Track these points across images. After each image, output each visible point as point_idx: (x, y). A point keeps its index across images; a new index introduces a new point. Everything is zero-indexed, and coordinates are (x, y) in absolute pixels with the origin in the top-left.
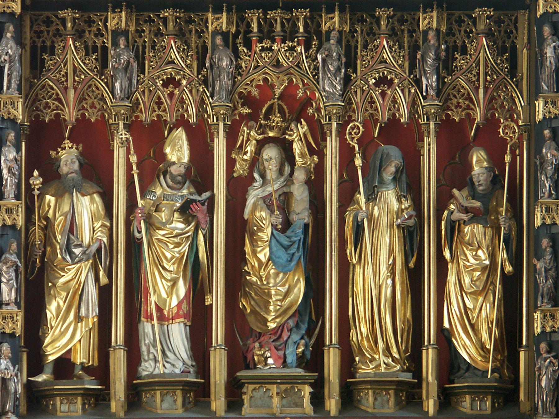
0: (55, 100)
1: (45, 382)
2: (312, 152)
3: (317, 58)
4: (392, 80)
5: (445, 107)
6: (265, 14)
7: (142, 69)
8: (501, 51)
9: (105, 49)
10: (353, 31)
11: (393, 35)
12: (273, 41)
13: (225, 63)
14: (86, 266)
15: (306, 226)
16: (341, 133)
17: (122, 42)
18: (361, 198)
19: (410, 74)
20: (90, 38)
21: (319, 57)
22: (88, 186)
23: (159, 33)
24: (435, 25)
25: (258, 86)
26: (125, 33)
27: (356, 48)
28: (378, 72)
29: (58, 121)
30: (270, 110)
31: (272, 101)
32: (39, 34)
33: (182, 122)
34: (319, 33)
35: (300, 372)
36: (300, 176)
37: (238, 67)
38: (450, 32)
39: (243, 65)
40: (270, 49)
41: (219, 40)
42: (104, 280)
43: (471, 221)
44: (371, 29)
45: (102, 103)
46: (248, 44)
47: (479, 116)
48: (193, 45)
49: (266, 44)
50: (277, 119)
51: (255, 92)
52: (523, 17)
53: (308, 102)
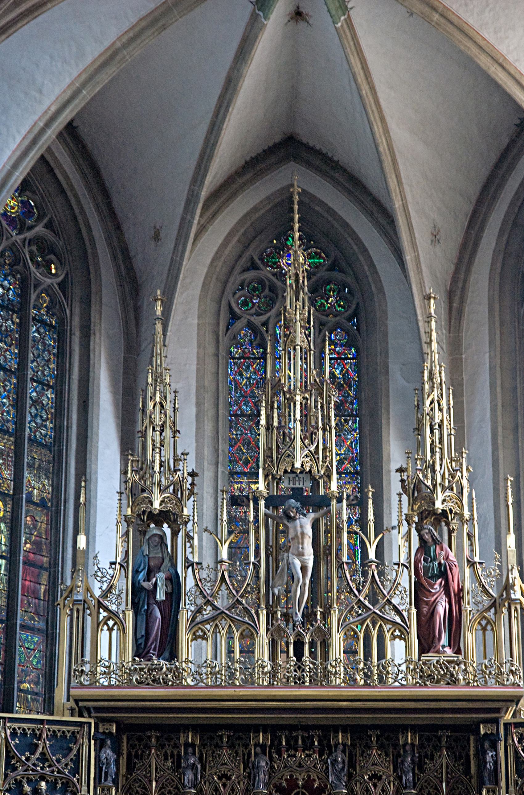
0: (142, 788)
3: (327, 762)
4: (381, 776)
6: (291, 733)
7: (204, 768)
8: (457, 759)
9: (179, 755)
11: (381, 747)
12: (296, 750)
13: (263, 763)
17: (190, 750)
19: (394, 772)
21: (329, 761)
24: (410, 741)
25: (286, 780)
26: (193, 745)
27: (356, 756)
28: (371, 771)
31: (298, 790)
32: (133, 747)
34: (329, 747)
37: (272, 767)
38: (422, 746)
39: (276, 766)
40: (294, 756)
41: (258, 749)
44: (367, 743)
45: (176, 790)
48: (241, 753)
49: (292, 752)
51: (284, 784)
52: (472, 738)
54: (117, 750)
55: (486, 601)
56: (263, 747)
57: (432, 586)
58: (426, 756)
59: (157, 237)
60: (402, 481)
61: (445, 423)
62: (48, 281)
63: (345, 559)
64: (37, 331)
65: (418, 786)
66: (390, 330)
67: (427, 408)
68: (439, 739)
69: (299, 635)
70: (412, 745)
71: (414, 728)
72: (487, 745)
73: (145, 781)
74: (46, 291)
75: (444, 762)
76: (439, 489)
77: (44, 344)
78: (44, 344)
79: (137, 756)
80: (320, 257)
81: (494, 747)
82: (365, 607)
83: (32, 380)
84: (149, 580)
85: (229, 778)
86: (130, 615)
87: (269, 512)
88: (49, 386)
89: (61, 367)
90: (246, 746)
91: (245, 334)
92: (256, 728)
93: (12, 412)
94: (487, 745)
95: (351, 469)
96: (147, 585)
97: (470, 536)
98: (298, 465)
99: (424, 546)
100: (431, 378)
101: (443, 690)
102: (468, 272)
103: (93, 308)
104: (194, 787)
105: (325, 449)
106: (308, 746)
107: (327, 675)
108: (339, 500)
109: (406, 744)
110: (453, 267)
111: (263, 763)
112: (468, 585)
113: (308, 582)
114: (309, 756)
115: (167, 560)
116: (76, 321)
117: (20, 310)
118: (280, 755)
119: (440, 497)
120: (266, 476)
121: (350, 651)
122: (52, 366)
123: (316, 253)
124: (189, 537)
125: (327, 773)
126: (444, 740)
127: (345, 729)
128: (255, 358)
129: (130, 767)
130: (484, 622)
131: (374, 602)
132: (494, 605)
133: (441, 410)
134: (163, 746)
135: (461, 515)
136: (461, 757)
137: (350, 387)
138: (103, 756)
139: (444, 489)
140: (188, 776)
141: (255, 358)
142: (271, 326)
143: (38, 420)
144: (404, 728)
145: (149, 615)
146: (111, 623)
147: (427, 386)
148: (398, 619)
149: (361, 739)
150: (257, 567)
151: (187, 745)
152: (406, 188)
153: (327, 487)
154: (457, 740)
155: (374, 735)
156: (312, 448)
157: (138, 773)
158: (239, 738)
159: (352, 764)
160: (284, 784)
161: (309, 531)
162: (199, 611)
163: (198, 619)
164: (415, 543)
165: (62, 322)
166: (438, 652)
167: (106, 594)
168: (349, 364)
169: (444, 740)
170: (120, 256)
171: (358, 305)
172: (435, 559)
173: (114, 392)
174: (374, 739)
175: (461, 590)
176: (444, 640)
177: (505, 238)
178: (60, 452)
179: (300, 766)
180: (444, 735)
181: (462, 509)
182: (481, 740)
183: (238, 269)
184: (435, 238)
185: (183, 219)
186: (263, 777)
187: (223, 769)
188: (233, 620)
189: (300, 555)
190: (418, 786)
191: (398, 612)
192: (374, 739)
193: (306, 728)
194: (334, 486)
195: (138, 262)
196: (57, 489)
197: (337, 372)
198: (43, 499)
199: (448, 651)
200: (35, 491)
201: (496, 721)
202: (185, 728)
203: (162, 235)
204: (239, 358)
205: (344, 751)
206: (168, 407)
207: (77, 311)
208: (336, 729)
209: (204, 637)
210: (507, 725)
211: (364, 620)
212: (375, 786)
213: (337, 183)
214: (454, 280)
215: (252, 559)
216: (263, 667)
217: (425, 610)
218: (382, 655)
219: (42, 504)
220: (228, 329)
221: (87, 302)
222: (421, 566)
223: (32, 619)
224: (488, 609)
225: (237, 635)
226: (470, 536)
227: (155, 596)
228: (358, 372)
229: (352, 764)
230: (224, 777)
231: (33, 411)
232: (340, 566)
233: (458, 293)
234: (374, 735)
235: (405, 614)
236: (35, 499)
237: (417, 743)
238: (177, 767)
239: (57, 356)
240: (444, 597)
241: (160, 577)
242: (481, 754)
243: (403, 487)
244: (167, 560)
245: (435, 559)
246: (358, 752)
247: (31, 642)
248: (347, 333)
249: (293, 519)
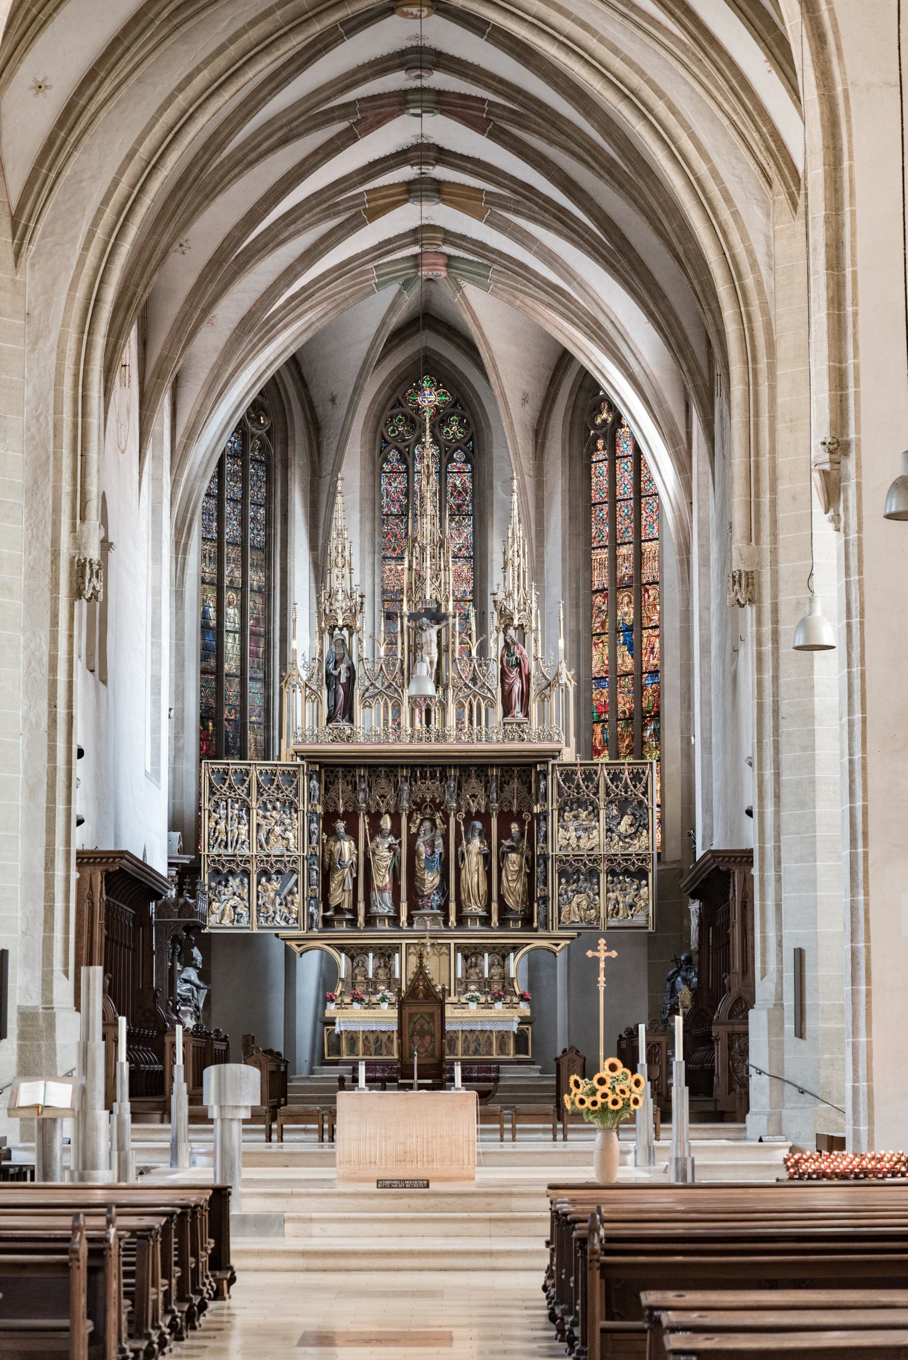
1: (331, 916)
2: (444, 823)
5: (500, 806)
8: (524, 783)
9: (355, 782)
10: (460, 775)
11: (478, 776)
13: (406, 788)
14: (347, 870)
15: (441, 854)
16: (455, 815)
18: (464, 842)
20: (349, 778)
22: (347, 837)
23: (378, 776)
26: (364, 777)
29: (336, 812)
30: (426, 807)
32: (328, 776)
33: (387, 812)
35: (439, 911)
36: (439, 832)
37: (411, 790)
38: (502, 776)
42: (355, 875)
43: (511, 852)
46: (416, 781)
47: (514, 809)
49: (423, 781)
50: (428, 811)
51: (419, 800)
52: (533, 771)
53: (441, 803)
54: (319, 781)
55: (544, 682)
56: (406, 778)
57: (511, 672)
58: (505, 782)
59: (333, 400)
60: (495, 602)
61: (522, 564)
62: (260, 432)
63: (457, 656)
64: (253, 467)
65: (499, 801)
66: (495, 456)
67: (510, 556)
68: (513, 771)
69: (428, 705)
70: (497, 776)
71: (497, 766)
72: (541, 777)
73: (335, 798)
74: (259, 438)
75: (515, 786)
76: (516, 611)
77: (258, 476)
78: (258, 476)
79: (330, 783)
80: (446, 396)
81: (545, 778)
82: (469, 687)
83: (252, 504)
84: (335, 669)
85: (385, 797)
86: (325, 692)
87: (410, 624)
88: (261, 506)
89: (268, 491)
90: (396, 776)
91: (393, 455)
92: (402, 766)
93: (240, 529)
94: (541, 777)
95: (467, 555)
96: (334, 673)
97: (536, 641)
98: (428, 597)
99: (507, 646)
100: (513, 534)
101: (516, 746)
102: (549, 417)
103: (289, 448)
104: (365, 802)
105: (445, 583)
106: (433, 777)
107: (444, 736)
108: (454, 617)
109: (492, 775)
110: (538, 414)
111: (406, 788)
112: (533, 672)
113: (434, 671)
114: (434, 783)
115: (346, 655)
116: (278, 457)
117: (242, 455)
118: (416, 781)
119: (516, 617)
120: (408, 601)
121: (459, 721)
122: (263, 490)
123: (444, 393)
124: (360, 641)
125: (444, 793)
126: (516, 772)
127: (455, 766)
128: (400, 473)
129: (327, 790)
130: (543, 696)
131: (475, 684)
132: (549, 685)
133: (518, 556)
134: (345, 776)
135: (531, 628)
136: (526, 783)
137: (467, 493)
138: (312, 785)
139: (519, 612)
140: (361, 796)
141: (400, 473)
142: (411, 449)
143: (255, 532)
144: (492, 766)
145: (336, 692)
146: (313, 697)
147: (510, 540)
148: (489, 695)
149: (465, 771)
150: (402, 662)
151: (360, 776)
152: (503, 378)
153: (447, 609)
154: (524, 771)
155: (473, 770)
156: (437, 584)
157: (332, 794)
158: (392, 771)
159: (460, 788)
160: (419, 800)
161: (435, 638)
162: (367, 690)
163: (366, 695)
164: (502, 644)
165: (268, 457)
166: (513, 716)
167: (309, 680)
168: (467, 477)
169: (516, 772)
170: (307, 406)
171: (472, 434)
172: (513, 655)
173: (305, 506)
174: (473, 772)
175: (529, 674)
176: (518, 708)
177: (574, 398)
178: (270, 552)
179: (428, 789)
180: (516, 769)
181: (531, 622)
182: (538, 773)
183: (389, 407)
184: (525, 400)
185: (352, 399)
186: (405, 796)
187: (382, 792)
188: (387, 696)
189: (429, 654)
190: (499, 801)
191: (489, 690)
192: (473, 772)
193: (432, 766)
194: (451, 609)
195: (319, 410)
196: (268, 579)
197: (458, 483)
198: (259, 587)
199: (520, 715)
200: (255, 583)
201: (546, 763)
202: (360, 766)
203: (336, 402)
204: (389, 473)
205: (455, 780)
206: (347, 554)
207: (278, 449)
208: (450, 766)
209: (370, 707)
210: (553, 765)
211: (468, 696)
212: (473, 801)
213: (458, 346)
214: (539, 422)
215: (399, 656)
216: (406, 731)
217: (507, 687)
218: (479, 723)
219: (259, 591)
220: (381, 452)
221: (286, 444)
222: (505, 659)
223: (256, 672)
224: (546, 688)
225: (390, 705)
226: (536, 641)
227: (339, 680)
228: (473, 482)
229: (460, 788)
230: (383, 796)
231: (252, 525)
232: (454, 661)
233: (542, 432)
234: (473, 770)
235: (494, 691)
236: (255, 588)
237: (499, 774)
238: (355, 789)
239: (266, 482)
240: (519, 680)
241: (343, 667)
242: (538, 782)
243: (495, 606)
244: (346, 655)
245: (513, 655)
246: (463, 780)
247: (256, 688)
248: (465, 453)
249: (425, 630)
